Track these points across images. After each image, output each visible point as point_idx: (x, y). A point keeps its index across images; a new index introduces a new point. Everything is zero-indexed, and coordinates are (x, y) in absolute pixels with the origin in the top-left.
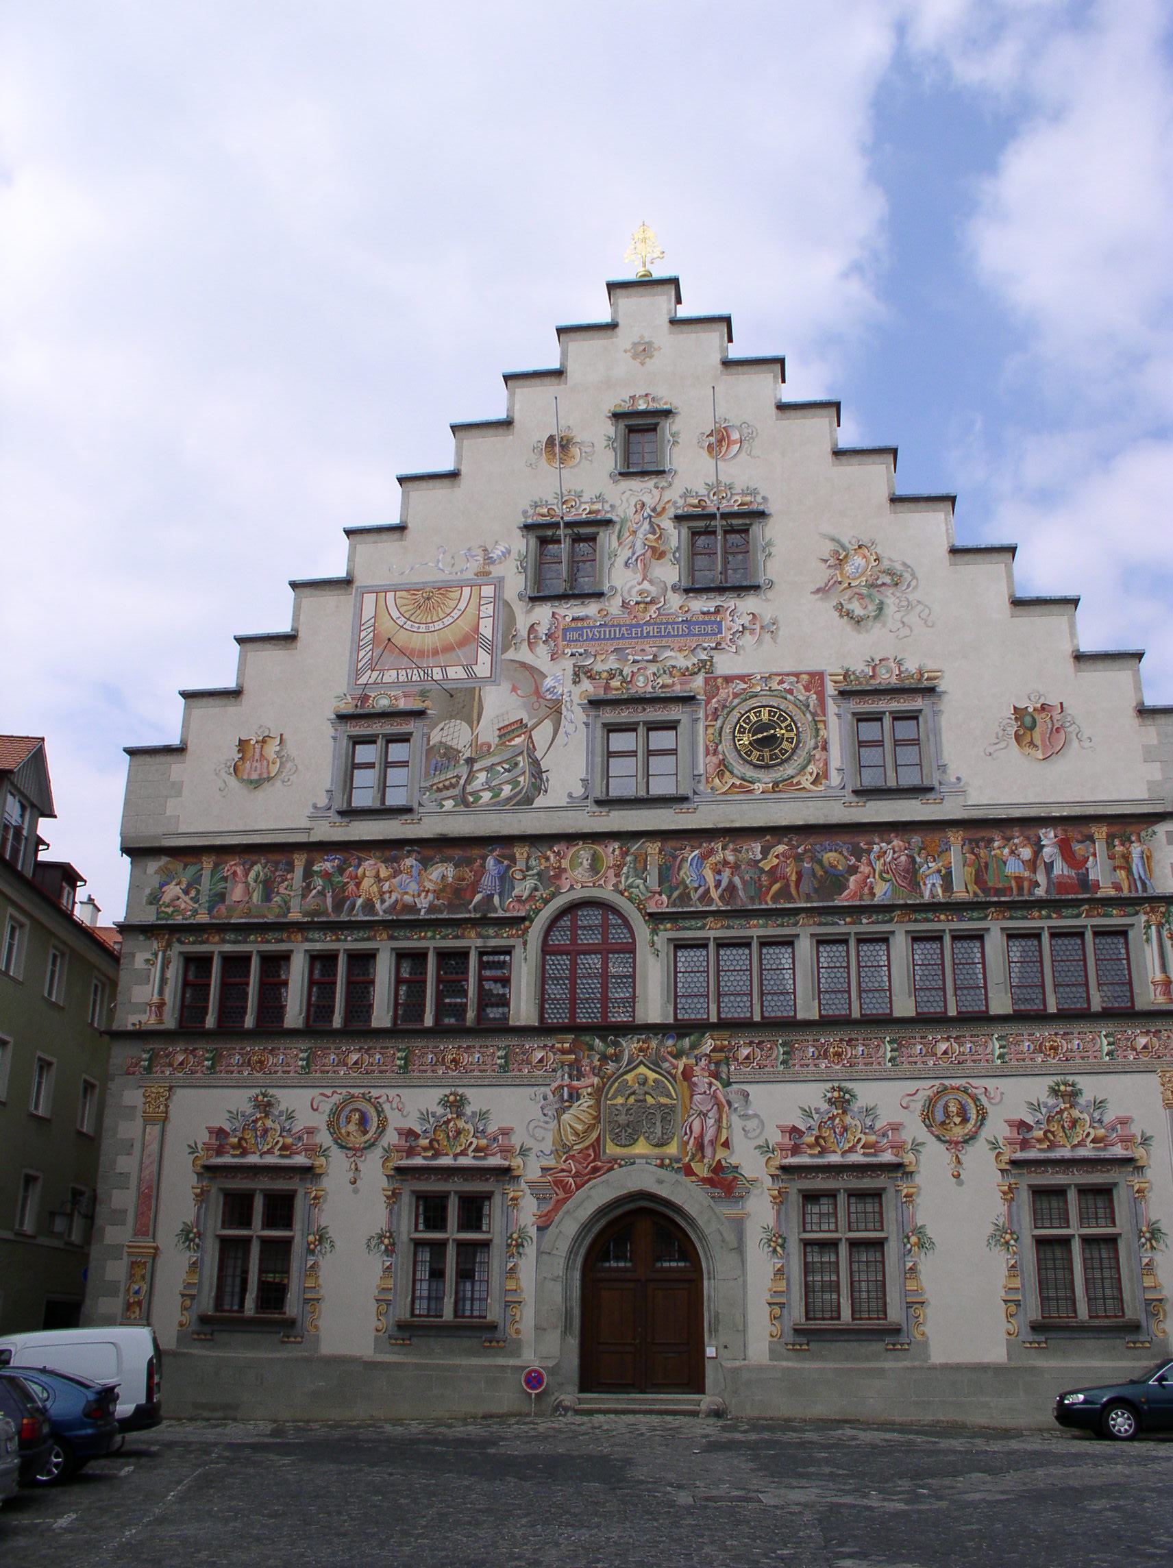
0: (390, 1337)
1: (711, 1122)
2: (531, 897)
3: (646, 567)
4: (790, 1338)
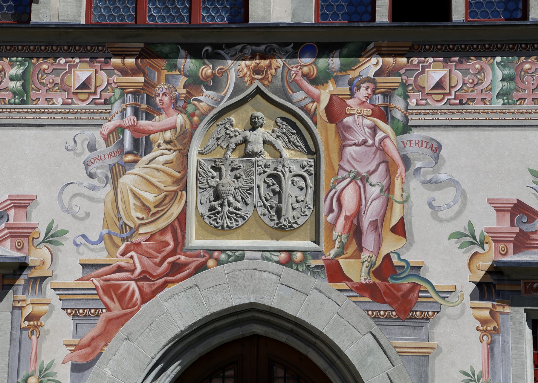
1: (374, 191)
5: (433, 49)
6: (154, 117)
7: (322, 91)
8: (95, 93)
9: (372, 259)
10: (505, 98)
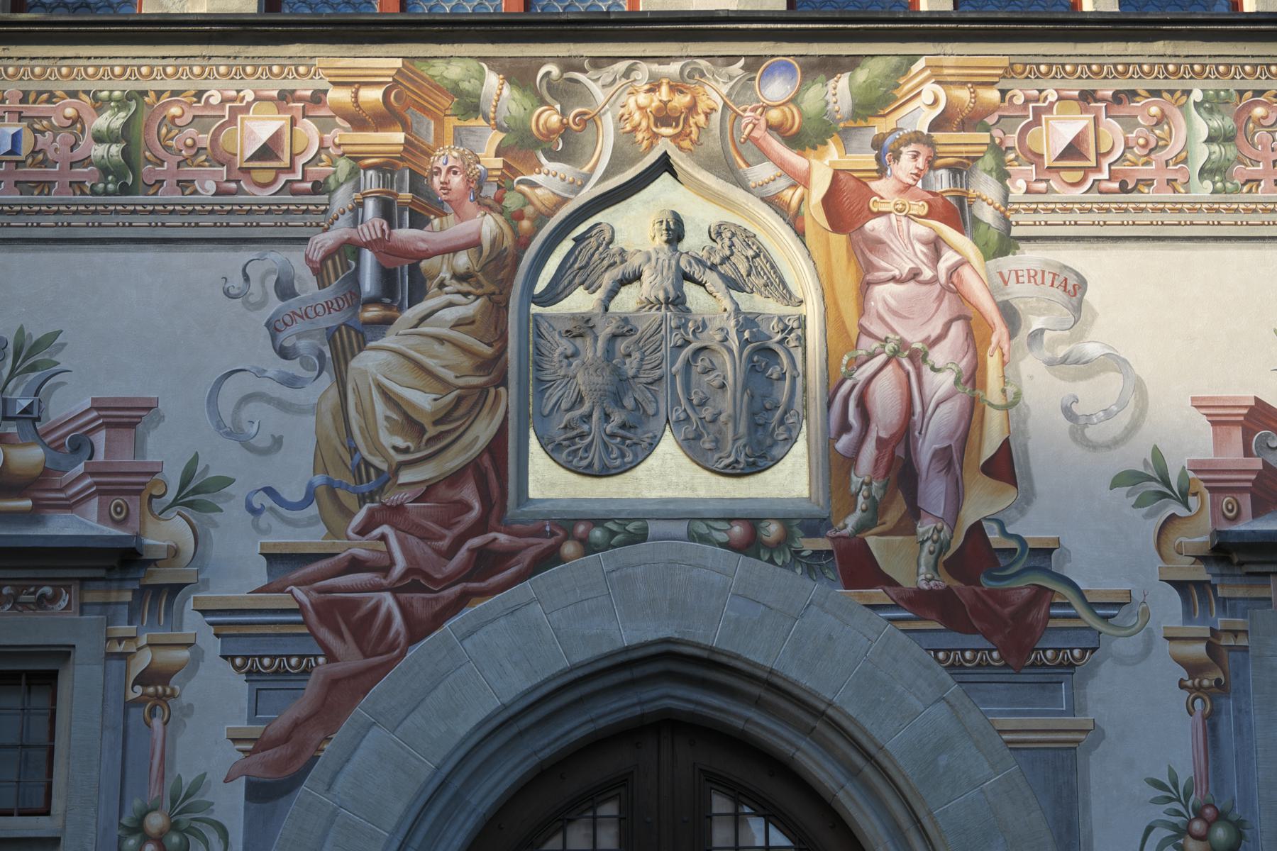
5: (1056, 73)
6: (428, 221)
7: (814, 161)
8: (291, 169)
9: (942, 533)
10: (1217, 178)
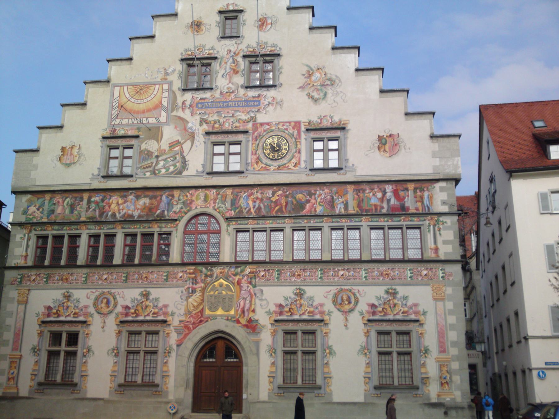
0: (115, 391)
1: (248, 302)
2: (180, 211)
3: (230, 77)
4: (276, 390)
